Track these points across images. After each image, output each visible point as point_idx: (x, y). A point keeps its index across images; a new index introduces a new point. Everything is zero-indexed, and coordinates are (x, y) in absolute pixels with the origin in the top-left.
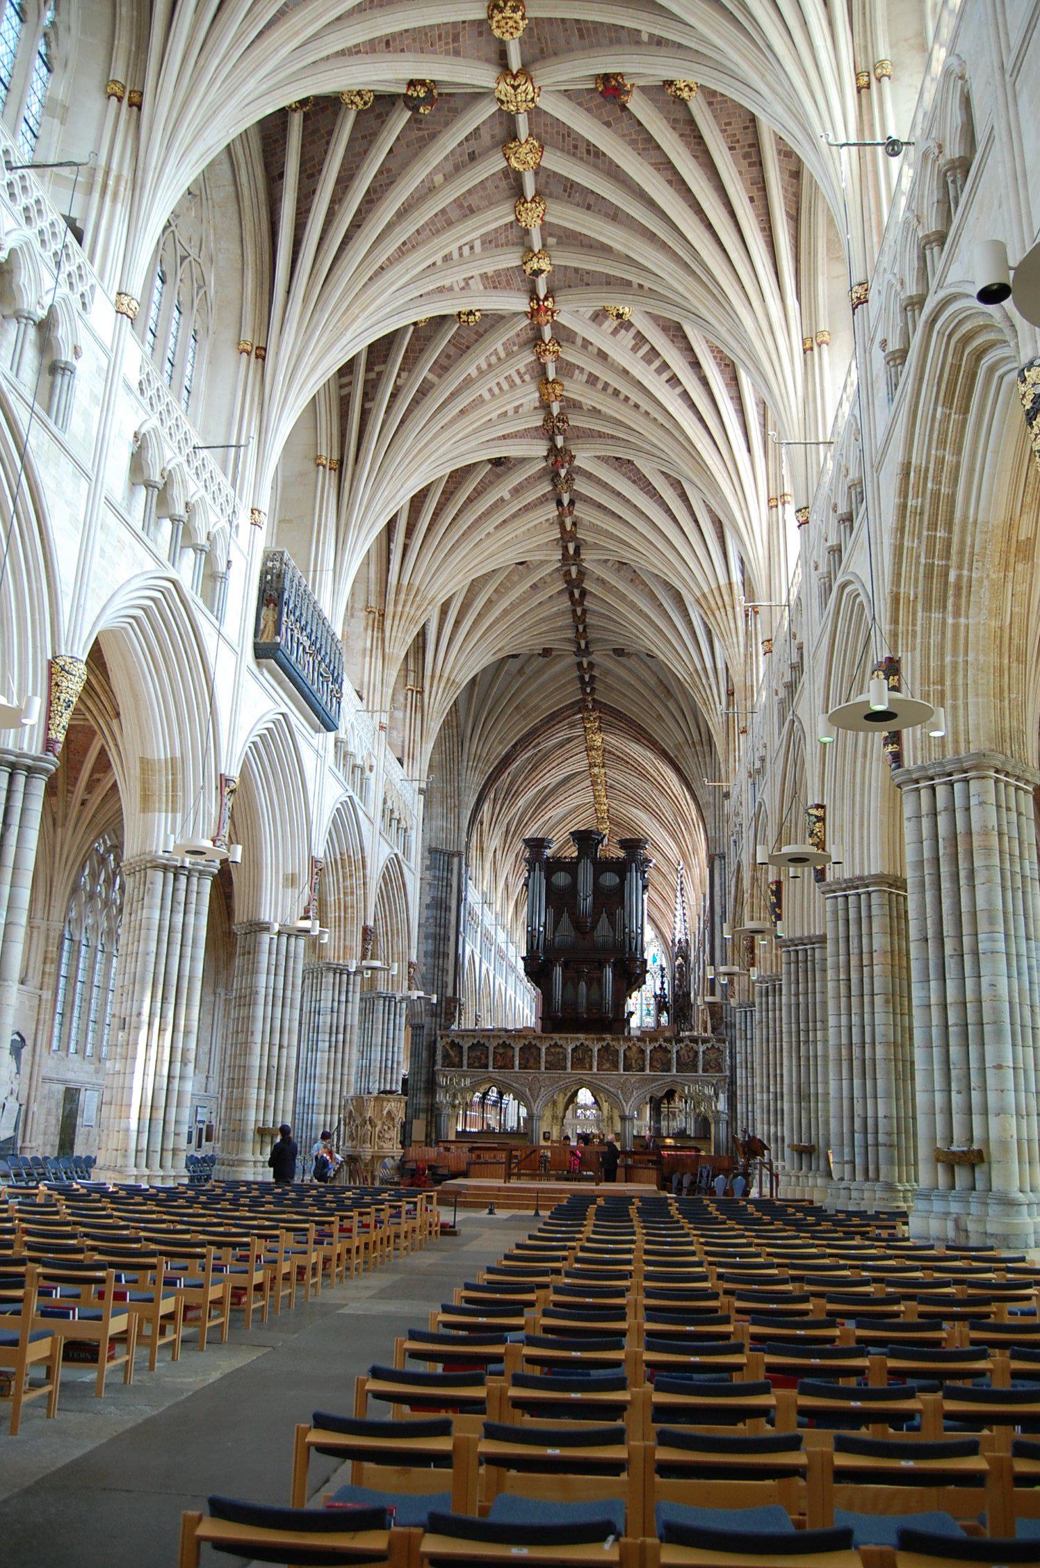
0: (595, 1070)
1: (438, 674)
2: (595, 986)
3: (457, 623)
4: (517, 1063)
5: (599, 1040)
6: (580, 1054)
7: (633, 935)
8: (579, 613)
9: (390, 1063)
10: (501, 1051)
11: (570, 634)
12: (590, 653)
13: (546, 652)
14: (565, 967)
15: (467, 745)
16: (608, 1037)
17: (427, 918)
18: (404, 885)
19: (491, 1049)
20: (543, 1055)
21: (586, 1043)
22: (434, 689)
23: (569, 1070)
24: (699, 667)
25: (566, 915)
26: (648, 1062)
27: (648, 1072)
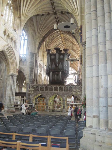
0: (58, 91)
1: (23, 13)
2: (58, 76)
3: (26, 3)
4: (44, 90)
5: (59, 86)
6: (56, 88)
7: (65, 66)
8: (52, 3)
9: (12, 89)
10: (41, 88)
11: (52, 9)
12: (57, 14)
13: (49, 14)
14: (53, 72)
15: (36, 34)
16: (61, 85)
17: (29, 65)
18: (14, 53)
19: (40, 87)
20: (49, 88)
21: (57, 86)
22: (23, 16)
23: (54, 91)
24: (74, 8)
25: (54, 63)
26: (68, 90)
27: (68, 91)
